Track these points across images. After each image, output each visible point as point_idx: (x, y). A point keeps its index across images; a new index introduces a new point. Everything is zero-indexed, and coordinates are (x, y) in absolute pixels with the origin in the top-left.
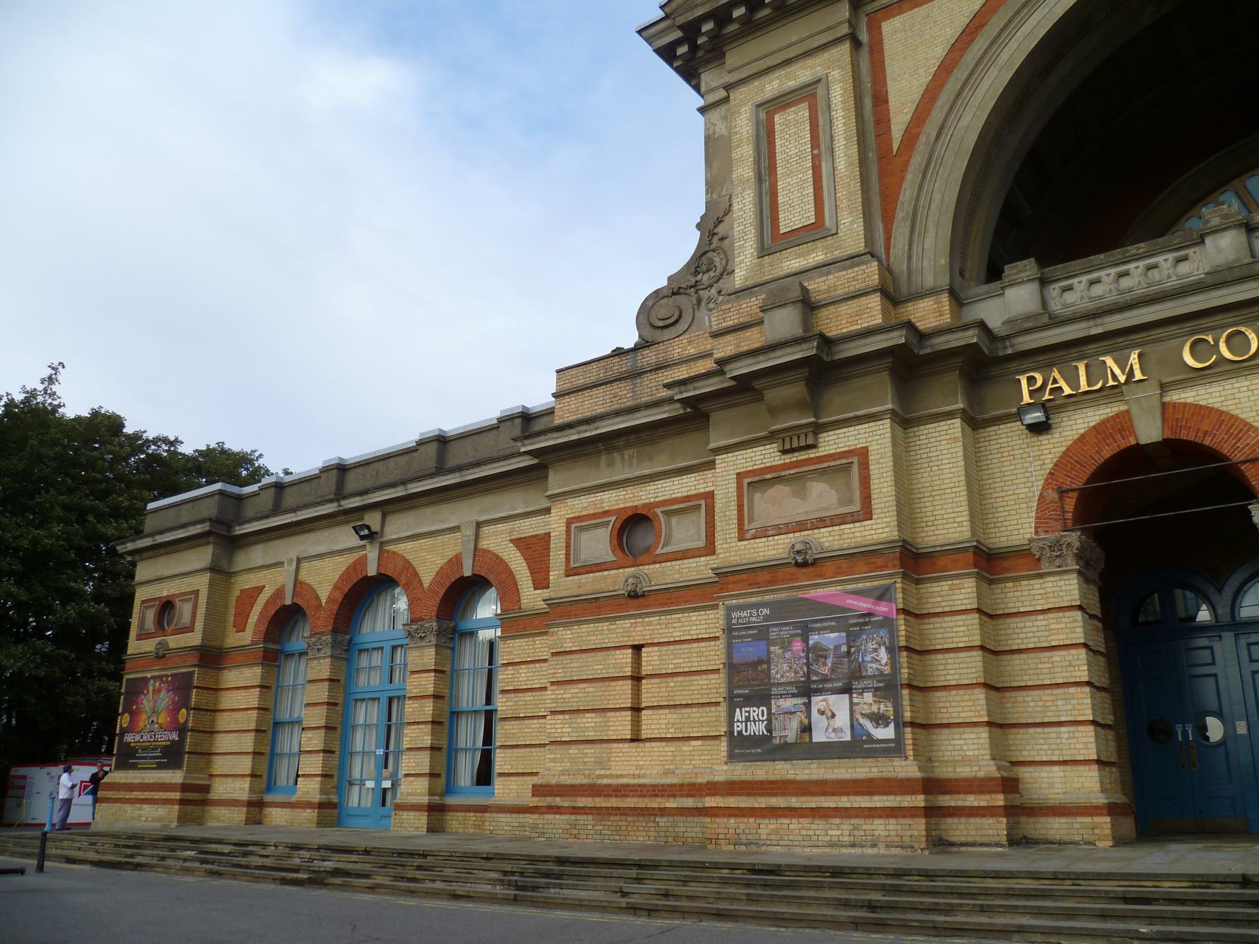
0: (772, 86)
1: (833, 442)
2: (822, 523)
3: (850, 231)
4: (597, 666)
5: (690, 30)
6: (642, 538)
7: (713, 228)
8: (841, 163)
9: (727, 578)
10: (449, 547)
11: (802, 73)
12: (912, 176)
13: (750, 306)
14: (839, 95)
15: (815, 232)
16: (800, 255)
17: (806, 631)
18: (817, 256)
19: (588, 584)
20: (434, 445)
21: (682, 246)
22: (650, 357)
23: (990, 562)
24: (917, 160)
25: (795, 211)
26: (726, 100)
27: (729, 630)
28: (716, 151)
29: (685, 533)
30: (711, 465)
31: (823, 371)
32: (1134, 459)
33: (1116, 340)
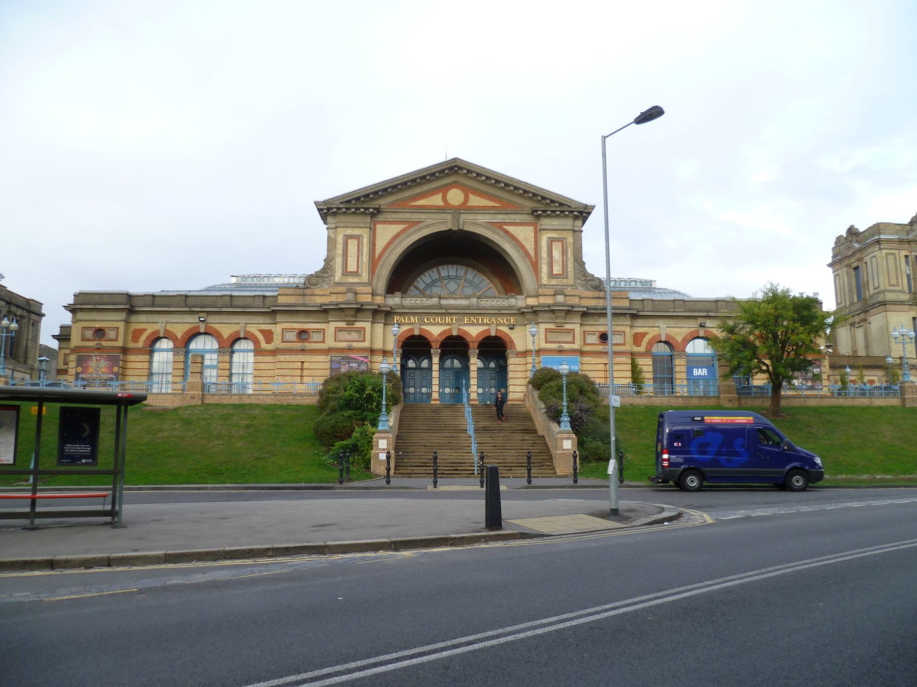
0: (349, 232)
1: (358, 325)
3: (365, 277)
4: (291, 366)
5: (329, 209)
6: (304, 336)
7: (329, 261)
8: (364, 260)
9: (329, 351)
10: (235, 328)
11: (357, 232)
12: (379, 267)
13: (342, 289)
14: (365, 241)
15: (356, 274)
17: (349, 363)
18: (356, 280)
19: (288, 345)
20: (228, 299)
21: (318, 265)
22: (308, 291)
23: (385, 353)
24: (380, 263)
25: (352, 267)
26: (336, 228)
27: (331, 361)
28: (331, 242)
29: (316, 337)
30: (328, 322)
31: (359, 310)
32: (413, 337)
33: (414, 314)
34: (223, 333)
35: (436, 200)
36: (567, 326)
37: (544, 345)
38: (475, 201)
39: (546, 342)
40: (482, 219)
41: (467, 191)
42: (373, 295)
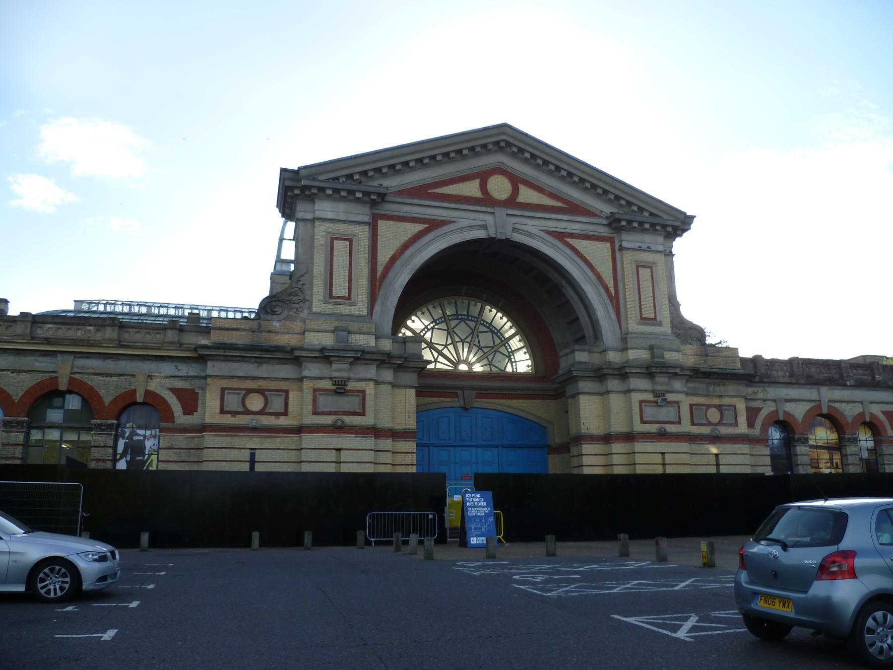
19: (228, 420)
34: (102, 392)
36: (670, 397)
37: (639, 427)
39: (642, 422)
42: (377, 338)
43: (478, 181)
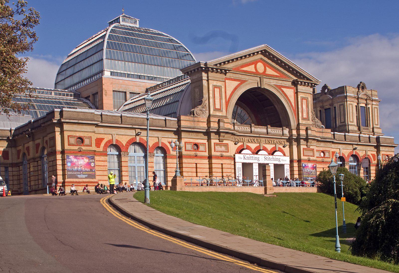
1: (225, 142)
2: (224, 152)
4: (191, 166)
16: (219, 113)
25: (218, 106)
35: (251, 68)
38: (270, 71)
40: (273, 82)
41: (266, 64)
43: (254, 65)
